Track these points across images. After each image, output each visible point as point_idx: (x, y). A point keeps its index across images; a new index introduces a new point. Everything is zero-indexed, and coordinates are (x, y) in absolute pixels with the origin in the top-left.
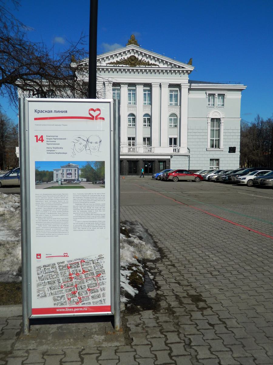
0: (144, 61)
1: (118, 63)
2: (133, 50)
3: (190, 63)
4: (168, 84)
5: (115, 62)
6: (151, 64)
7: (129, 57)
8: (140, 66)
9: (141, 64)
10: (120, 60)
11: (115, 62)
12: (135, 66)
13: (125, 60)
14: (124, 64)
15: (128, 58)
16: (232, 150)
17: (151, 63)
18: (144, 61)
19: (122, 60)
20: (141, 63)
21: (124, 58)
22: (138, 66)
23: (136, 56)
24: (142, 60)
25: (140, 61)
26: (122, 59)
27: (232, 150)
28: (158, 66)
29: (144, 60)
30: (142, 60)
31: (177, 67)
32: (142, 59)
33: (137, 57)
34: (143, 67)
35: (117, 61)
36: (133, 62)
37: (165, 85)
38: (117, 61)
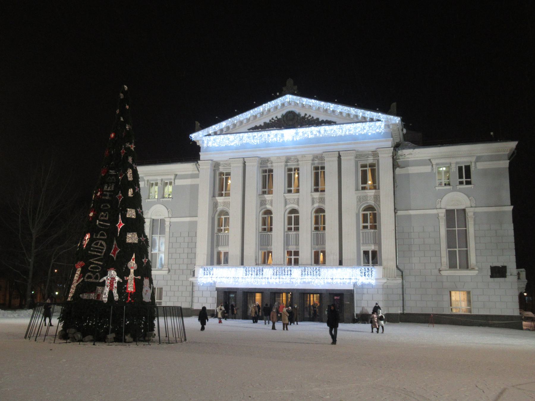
5: (263, 125)
10: (270, 121)
11: (263, 125)
16: (498, 272)
18: (309, 118)
21: (276, 117)
24: (306, 117)
25: (304, 118)
26: (272, 119)
27: (498, 272)
29: (310, 116)
30: (306, 117)
32: (306, 115)
36: (292, 120)
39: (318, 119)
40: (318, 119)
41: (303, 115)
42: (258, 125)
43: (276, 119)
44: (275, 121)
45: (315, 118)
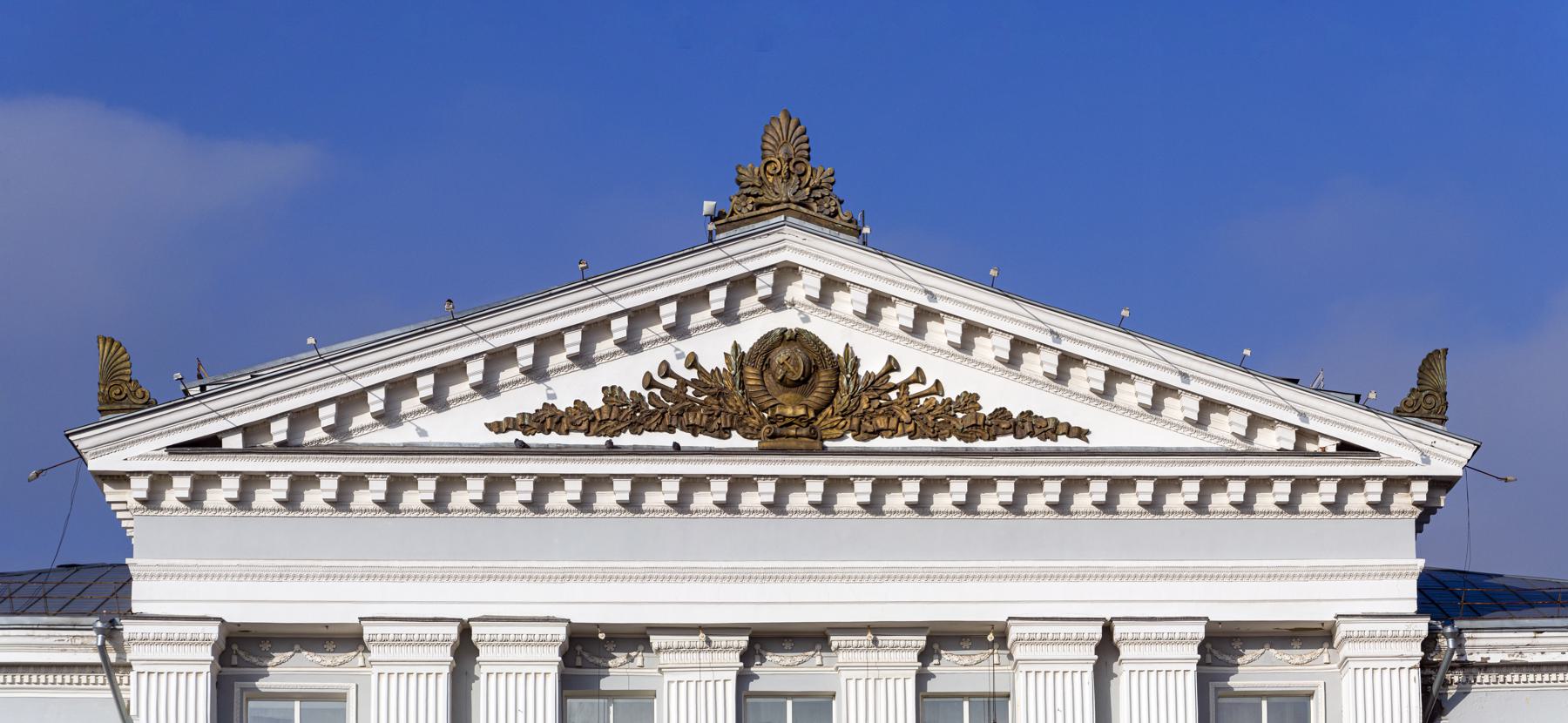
0: (914, 389)
1: (623, 413)
2: (786, 272)
3: (1425, 404)
4: (1199, 631)
5: (596, 402)
6: (1001, 422)
7: (746, 348)
8: (879, 443)
9: (881, 422)
10: (650, 383)
11: (596, 402)
12: (812, 442)
13: (707, 382)
14: (694, 430)
15: (739, 359)
17: (1001, 413)
18: (914, 389)
19: (671, 383)
20: (878, 406)
21: (693, 363)
22: (850, 442)
23: (833, 333)
24: (895, 378)
25: (877, 384)
26: (667, 371)
28: (1082, 434)
30: (895, 378)
31: (1288, 440)
32: (892, 366)
33: (838, 350)
34: (904, 458)
35: (611, 393)
37: (1159, 641)
38: (611, 393)
39: (970, 400)
40: (970, 400)
41: (871, 365)
42: (563, 404)
43: (692, 375)
44: (683, 383)
45: (952, 392)
